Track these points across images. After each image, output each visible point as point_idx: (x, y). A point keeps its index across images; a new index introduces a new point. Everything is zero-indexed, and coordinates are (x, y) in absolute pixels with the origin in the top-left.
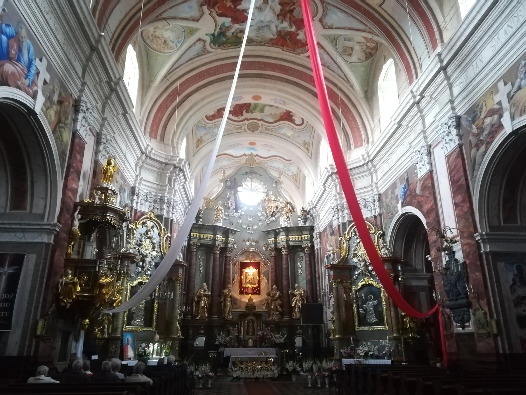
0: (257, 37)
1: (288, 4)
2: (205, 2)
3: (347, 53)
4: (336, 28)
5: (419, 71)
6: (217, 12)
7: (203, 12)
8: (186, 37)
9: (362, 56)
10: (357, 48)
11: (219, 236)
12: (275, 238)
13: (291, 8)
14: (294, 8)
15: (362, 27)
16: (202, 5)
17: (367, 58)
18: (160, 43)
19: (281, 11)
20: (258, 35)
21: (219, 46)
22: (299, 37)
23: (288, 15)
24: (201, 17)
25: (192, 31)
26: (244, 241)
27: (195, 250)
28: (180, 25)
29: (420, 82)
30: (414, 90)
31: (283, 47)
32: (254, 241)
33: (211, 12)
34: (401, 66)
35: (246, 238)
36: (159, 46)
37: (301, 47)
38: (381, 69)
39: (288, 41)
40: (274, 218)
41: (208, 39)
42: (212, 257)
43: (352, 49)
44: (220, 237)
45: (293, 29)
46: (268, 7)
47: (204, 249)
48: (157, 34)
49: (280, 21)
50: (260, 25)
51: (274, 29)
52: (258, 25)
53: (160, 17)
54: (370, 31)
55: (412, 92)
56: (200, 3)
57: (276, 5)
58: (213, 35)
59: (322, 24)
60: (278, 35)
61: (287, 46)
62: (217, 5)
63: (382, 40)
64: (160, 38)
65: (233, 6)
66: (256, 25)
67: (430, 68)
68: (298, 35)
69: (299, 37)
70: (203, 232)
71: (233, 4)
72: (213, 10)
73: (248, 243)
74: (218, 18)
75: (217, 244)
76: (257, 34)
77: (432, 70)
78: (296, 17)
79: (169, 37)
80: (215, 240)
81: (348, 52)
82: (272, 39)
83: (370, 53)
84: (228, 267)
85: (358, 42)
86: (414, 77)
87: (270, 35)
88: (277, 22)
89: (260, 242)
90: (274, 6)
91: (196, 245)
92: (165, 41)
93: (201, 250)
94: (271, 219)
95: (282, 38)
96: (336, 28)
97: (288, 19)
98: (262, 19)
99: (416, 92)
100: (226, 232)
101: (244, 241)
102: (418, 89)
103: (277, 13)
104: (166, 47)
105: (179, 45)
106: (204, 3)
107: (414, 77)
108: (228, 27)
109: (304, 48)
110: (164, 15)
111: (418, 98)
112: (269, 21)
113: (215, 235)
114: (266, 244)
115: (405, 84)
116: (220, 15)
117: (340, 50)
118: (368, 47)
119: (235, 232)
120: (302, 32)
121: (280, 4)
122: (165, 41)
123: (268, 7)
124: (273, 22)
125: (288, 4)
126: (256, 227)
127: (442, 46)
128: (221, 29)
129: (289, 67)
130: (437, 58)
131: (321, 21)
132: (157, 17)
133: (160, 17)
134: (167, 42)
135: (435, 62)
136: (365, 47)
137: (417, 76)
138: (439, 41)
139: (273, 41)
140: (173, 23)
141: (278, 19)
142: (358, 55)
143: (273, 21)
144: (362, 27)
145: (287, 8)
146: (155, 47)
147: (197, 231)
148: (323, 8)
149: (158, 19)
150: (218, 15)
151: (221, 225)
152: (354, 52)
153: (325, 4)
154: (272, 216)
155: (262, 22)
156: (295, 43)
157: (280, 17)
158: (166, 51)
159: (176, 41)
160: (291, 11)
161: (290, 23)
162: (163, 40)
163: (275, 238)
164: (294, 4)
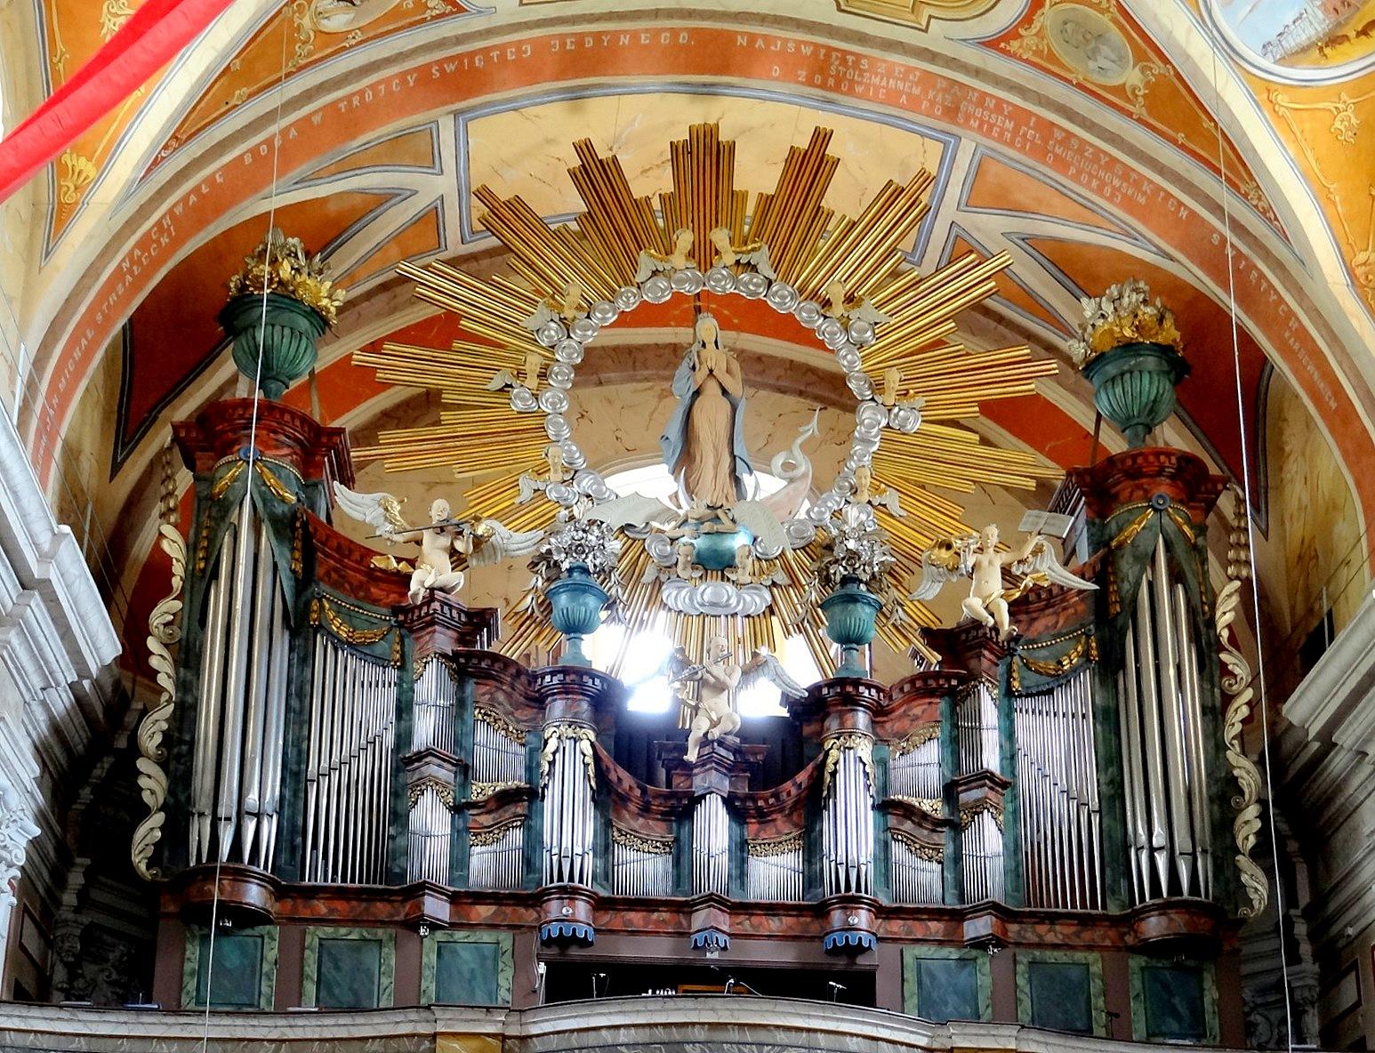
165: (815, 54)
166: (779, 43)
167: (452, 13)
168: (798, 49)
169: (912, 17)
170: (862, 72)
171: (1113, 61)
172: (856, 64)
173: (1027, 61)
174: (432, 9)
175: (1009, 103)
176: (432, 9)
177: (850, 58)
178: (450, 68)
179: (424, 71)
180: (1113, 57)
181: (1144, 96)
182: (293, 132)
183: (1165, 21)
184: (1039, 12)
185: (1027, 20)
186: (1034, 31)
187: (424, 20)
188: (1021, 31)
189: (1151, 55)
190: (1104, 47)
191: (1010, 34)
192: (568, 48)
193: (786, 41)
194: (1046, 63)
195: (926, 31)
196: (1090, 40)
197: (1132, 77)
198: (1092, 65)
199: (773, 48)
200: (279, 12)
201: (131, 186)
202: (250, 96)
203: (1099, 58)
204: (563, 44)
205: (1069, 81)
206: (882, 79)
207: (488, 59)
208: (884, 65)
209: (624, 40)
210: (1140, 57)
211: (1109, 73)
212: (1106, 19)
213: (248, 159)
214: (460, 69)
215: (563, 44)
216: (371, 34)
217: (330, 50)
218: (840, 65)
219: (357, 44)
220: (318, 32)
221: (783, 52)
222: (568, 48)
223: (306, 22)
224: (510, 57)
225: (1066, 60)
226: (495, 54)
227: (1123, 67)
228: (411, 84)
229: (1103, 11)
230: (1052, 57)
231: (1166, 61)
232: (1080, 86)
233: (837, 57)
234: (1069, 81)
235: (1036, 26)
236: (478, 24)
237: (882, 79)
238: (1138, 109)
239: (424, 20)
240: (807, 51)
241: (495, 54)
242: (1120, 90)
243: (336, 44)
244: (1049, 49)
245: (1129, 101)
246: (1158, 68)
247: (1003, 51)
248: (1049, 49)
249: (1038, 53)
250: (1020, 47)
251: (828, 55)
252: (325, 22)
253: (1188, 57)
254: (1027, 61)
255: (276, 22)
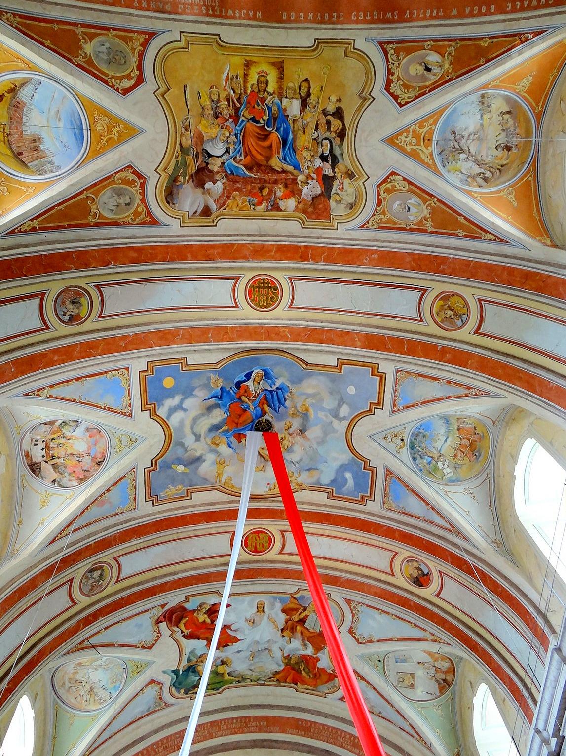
0: (250, 670)
1: (297, 610)
2: (164, 617)
3: (406, 683)
4: (379, 641)
5: (534, 690)
6: (182, 632)
7: (159, 632)
8: (129, 678)
9: (434, 688)
10: (420, 673)
13: (302, 616)
14: (307, 616)
15: (418, 633)
16: (158, 622)
17: (442, 690)
18: (83, 693)
19: (286, 622)
20: (252, 668)
21: (186, 692)
22: (320, 665)
23: (298, 627)
24: (156, 641)
25: (140, 668)
28: (119, 658)
29: (544, 710)
30: (541, 727)
31: (296, 685)
33: (173, 631)
34: (503, 691)
36: (79, 699)
37: (327, 682)
38: (471, 707)
39: (303, 672)
41: (167, 680)
43: (413, 675)
45: (310, 651)
46: (266, 618)
48: (79, 677)
49: (286, 638)
50: (255, 648)
51: (278, 655)
52: (251, 649)
53: (86, 644)
54: (434, 638)
55: (537, 731)
56: (156, 618)
57: (277, 614)
58: (176, 672)
59: (355, 638)
60: (287, 664)
61: (303, 682)
62: (184, 621)
63: (458, 650)
64: (84, 684)
65: (208, 621)
66: (248, 648)
67: (551, 678)
68: (318, 660)
69: (320, 665)
71: (209, 616)
72: (176, 629)
74: (184, 642)
76: (251, 665)
77: (557, 681)
78: (312, 630)
79: (100, 681)
81: (406, 682)
82: (277, 673)
83: (445, 681)
85: (419, 663)
86: (530, 702)
87: (273, 664)
88: (281, 642)
90: (274, 616)
92: (92, 689)
95: (293, 669)
96: (379, 641)
97: (298, 635)
98: (257, 638)
99: (545, 730)
102: (546, 722)
103: (281, 625)
104: (92, 699)
105: (115, 695)
106: (162, 618)
107: (530, 702)
108: (201, 656)
109: (332, 683)
110: (93, 641)
111: (554, 741)
112: (269, 641)
115: (520, 722)
116: (188, 637)
117: (392, 679)
118: (438, 670)
120: (324, 654)
121: (284, 611)
122: (92, 689)
123: (266, 618)
124: (276, 642)
125: (297, 610)
127: (556, 637)
128: (189, 660)
129: (312, 722)
130: (556, 656)
131: (351, 631)
132: (80, 644)
133: (86, 644)
134: (95, 691)
135: (554, 663)
136: (433, 671)
137: (535, 702)
138: (547, 631)
139: (278, 676)
140: (106, 655)
141: (283, 636)
142: (424, 687)
143: (277, 640)
144: (418, 633)
145: (296, 618)
146: (73, 700)
148: (352, 611)
149: (81, 647)
150: (184, 636)
152: (418, 683)
153: (353, 605)
155: (257, 643)
156: (315, 675)
157: (287, 633)
158: (92, 707)
159: (110, 687)
160: (302, 621)
161: (303, 640)
162: (88, 687)
164: (305, 609)
165: (226, 12)
166: (243, 16)
167: (385, 43)
168: (234, 13)
169: (188, 39)
170: (204, 5)
171: (99, 52)
172: (207, 10)
173: (134, 32)
174: (392, 49)
175: (136, 8)
176: (392, 49)
177: (211, 12)
178: (389, 15)
179: (401, 20)
180: (100, 55)
181: (80, 40)
182: (468, 10)
183: (86, 86)
184: (137, 63)
185: (141, 56)
186: (136, 51)
187: (398, 43)
188: (141, 48)
189: (86, 65)
190: (106, 58)
191: (145, 44)
192: (335, 14)
193: (240, 18)
194: (126, 34)
195: (181, 32)
196: (116, 58)
197: (89, 48)
198: (107, 45)
199: (245, 12)
200: (458, 77)
201: (550, 33)
202: (481, 39)
203: (106, 51)
204: (338, 17)
205: (114, 29)
206: (195, 2)
207: (372, 15)
208: (195, 11)
209: (311, 16)
210: (90, 62)
211: (99, 44)
212: (111, 73)
213: (493, 8)
214: (385, 15)
215: (338, 17)
216: (420, 44)
217: (441, 43)
218: (215, 6)
219: (426, 41)
220: (443, 56)
221: (240, 11)
222: (335, 14)
223: (447, 65)
224: (361, 14)
225: (118, 41)
226: (368, 18)
227: (94, 51)
228: (408, 12)
229: (113, 77)
230: (124, 39)
231: (79, 66)
232: (108, 29)
233: (216, 11)
234: (114, 29)
235: (136, 55)
236: (374, 34)
237: (195, 2)
238: (80, 30)
239: (398, 43)
240: (231, 13)
241: (368, 18)
242: (92, 37)
243: (437, 45)
244: (127, 44)
245: (85, 33)
246: (80, 60)
247: (144, 33)
248: (127, 44)
249: (131, 39)
250: (139, 39)
251: (221, 11)
252: (440, 61)
253: (71, 74)
254: (134, 32)
255: (460, 73)
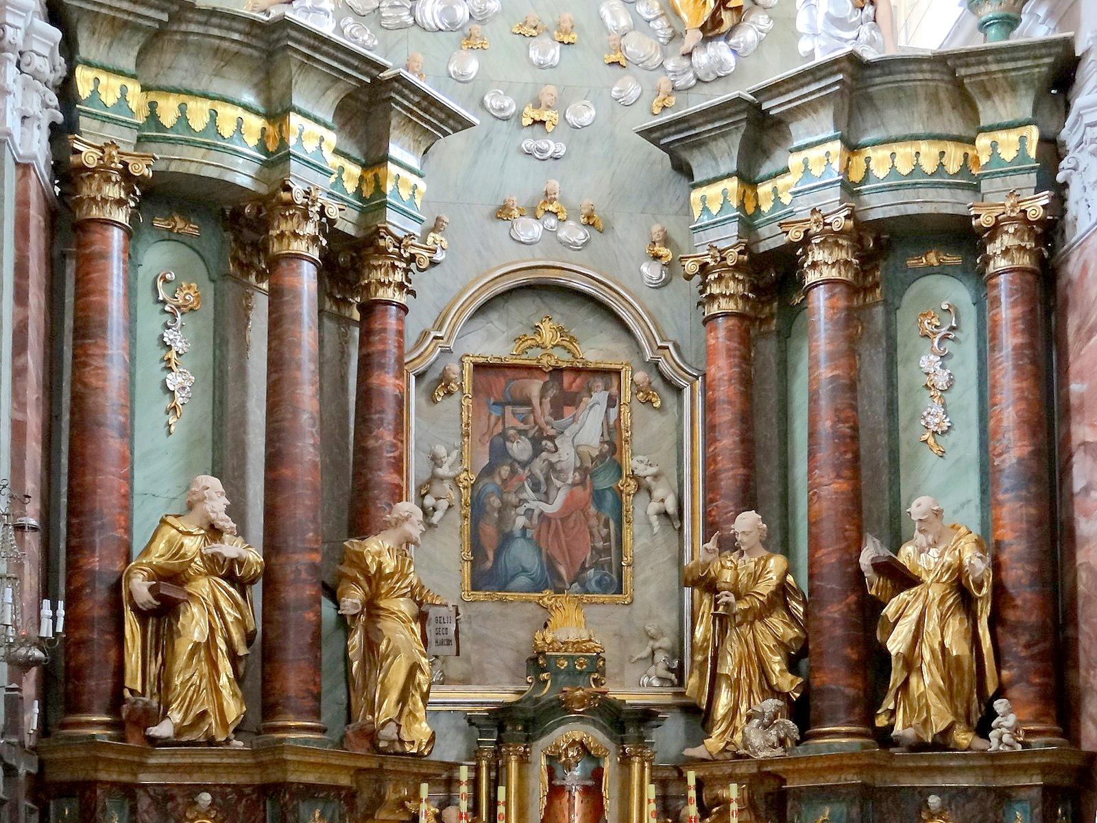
11: (310, 126)
12: (748, 180)
26: (502, 213)
27: (121, 216)
32: (573, 213)
35: (520, 183)
40: (720, 50)
42: (261, 303)
44: (315, 137)
47: (192, 229)
70: (174, 80)
73: (531, 230)
75: (298, 190)
80: (276, 158)
84: (387, 381)
89: (620, 225)
91: (126, 175)
93: (170, 236)
94: (702, 59)
100: (374, 104)
101: (502, 213)
113: (276, 113)
114: (666, 242)
119: (436, 120)
126: (588, 116)
147: (129, 63)
151: (326, 28)
154: (711, 30)
163: (748, 180)
